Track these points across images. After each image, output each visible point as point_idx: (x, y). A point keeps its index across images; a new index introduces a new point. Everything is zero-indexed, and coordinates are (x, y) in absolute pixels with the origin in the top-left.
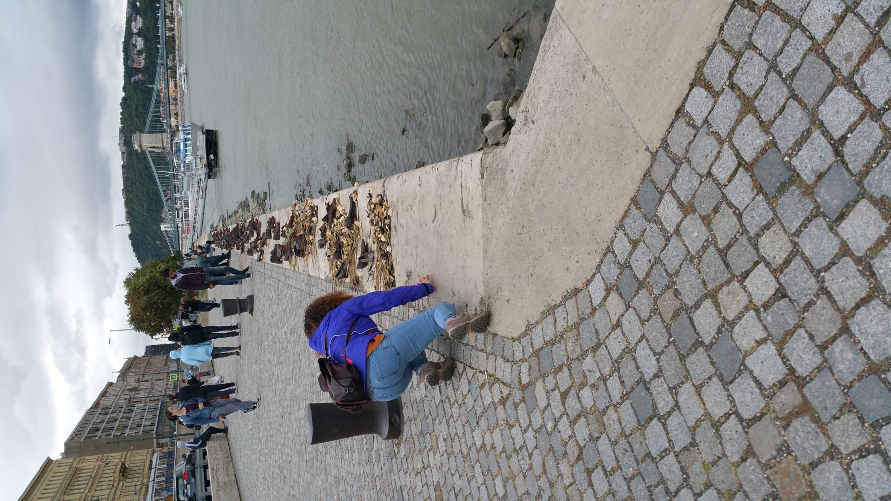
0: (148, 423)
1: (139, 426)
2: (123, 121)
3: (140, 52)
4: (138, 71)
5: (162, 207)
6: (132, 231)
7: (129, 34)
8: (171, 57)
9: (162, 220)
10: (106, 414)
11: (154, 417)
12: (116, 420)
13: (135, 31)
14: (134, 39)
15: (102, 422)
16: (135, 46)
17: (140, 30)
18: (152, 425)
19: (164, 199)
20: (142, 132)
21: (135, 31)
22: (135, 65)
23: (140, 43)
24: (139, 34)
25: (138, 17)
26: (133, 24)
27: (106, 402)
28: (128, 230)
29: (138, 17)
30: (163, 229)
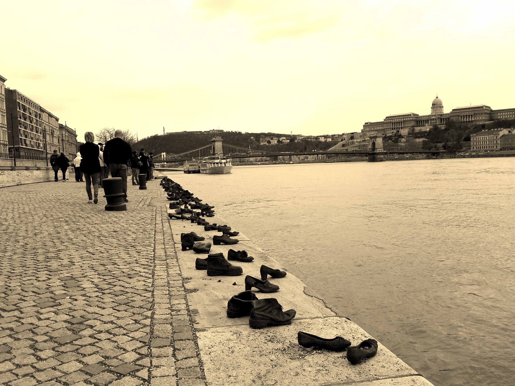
0: (28, 142)
1: (26, 137)
2: (228, 133)
3: (269, 142)
4: (258, 141)
5: (176, 153)
6: (161, 136)
7: (279, 136)
8: (268, 159)
9: (168, 153)
10: (36, 116)
11: (32, 146)
12: (31, 122)
13: (281, 139)
14: (276, 138)
15: (30, 114)
16: (272, 139)
17: (282, 142)
18: (26, 145)
19: (182, 154)
20: (223, 142)
21: (281, 139)
22: (261, 139)
23: (274, 142)
24: (279, 141)
25: (288, 141)
26: (284, 138)
27: (45, 116)
28: (160, 133)
29: (288, 141)
30: (162, 154)
